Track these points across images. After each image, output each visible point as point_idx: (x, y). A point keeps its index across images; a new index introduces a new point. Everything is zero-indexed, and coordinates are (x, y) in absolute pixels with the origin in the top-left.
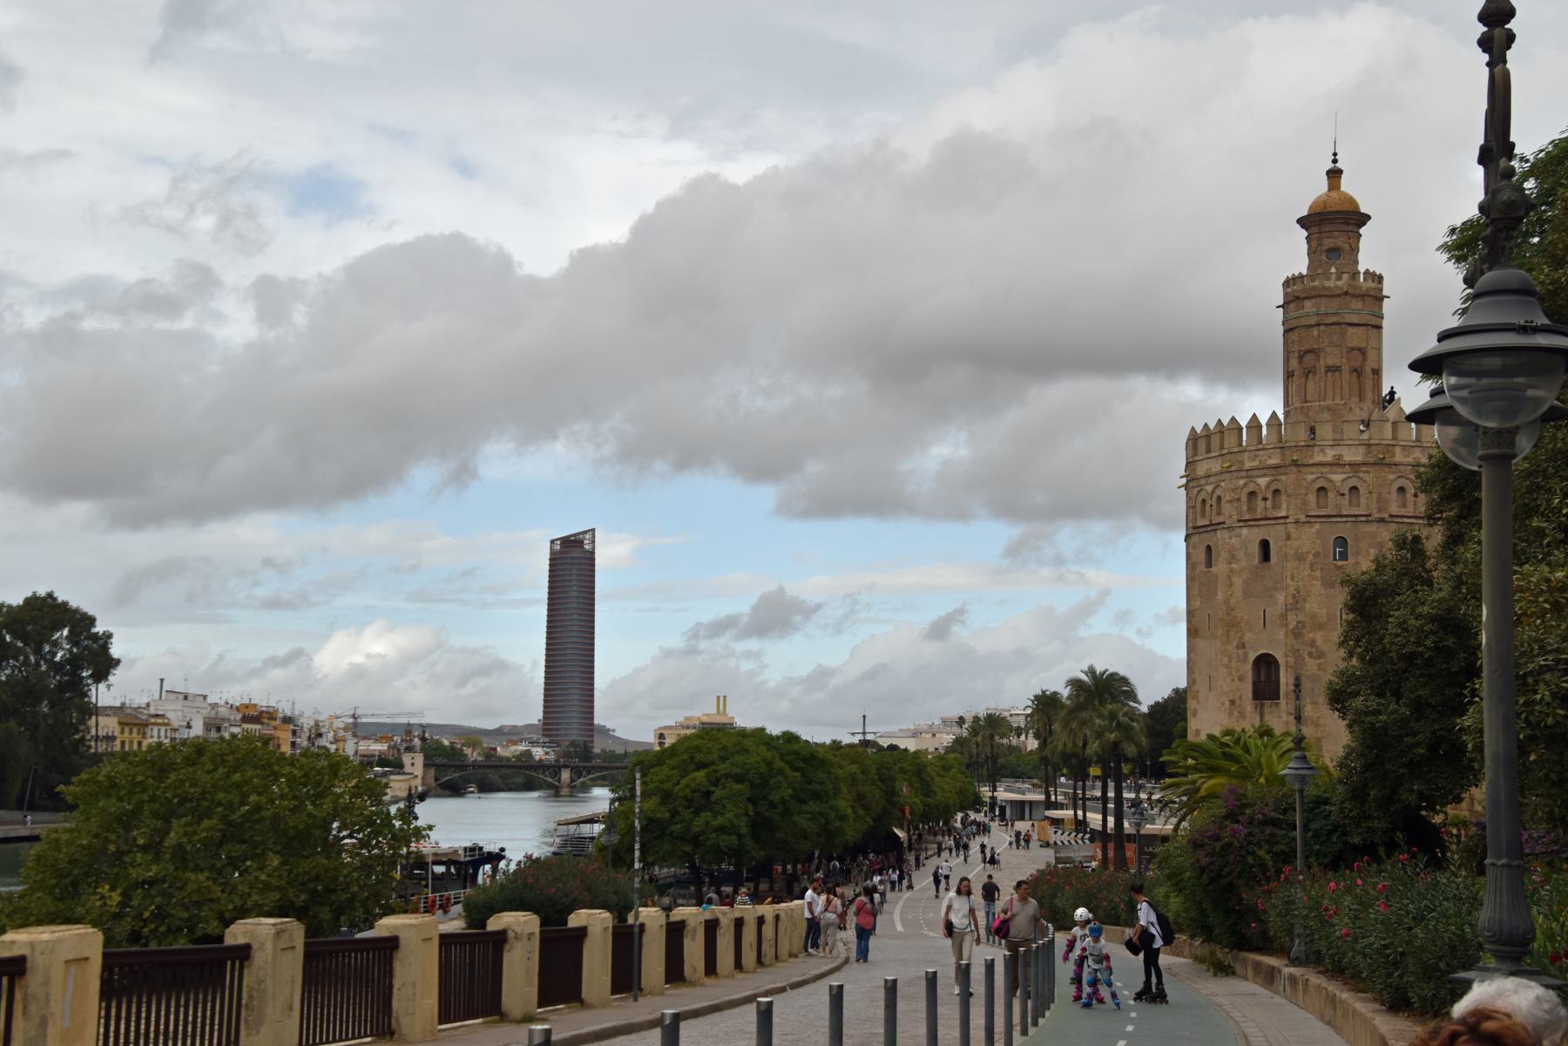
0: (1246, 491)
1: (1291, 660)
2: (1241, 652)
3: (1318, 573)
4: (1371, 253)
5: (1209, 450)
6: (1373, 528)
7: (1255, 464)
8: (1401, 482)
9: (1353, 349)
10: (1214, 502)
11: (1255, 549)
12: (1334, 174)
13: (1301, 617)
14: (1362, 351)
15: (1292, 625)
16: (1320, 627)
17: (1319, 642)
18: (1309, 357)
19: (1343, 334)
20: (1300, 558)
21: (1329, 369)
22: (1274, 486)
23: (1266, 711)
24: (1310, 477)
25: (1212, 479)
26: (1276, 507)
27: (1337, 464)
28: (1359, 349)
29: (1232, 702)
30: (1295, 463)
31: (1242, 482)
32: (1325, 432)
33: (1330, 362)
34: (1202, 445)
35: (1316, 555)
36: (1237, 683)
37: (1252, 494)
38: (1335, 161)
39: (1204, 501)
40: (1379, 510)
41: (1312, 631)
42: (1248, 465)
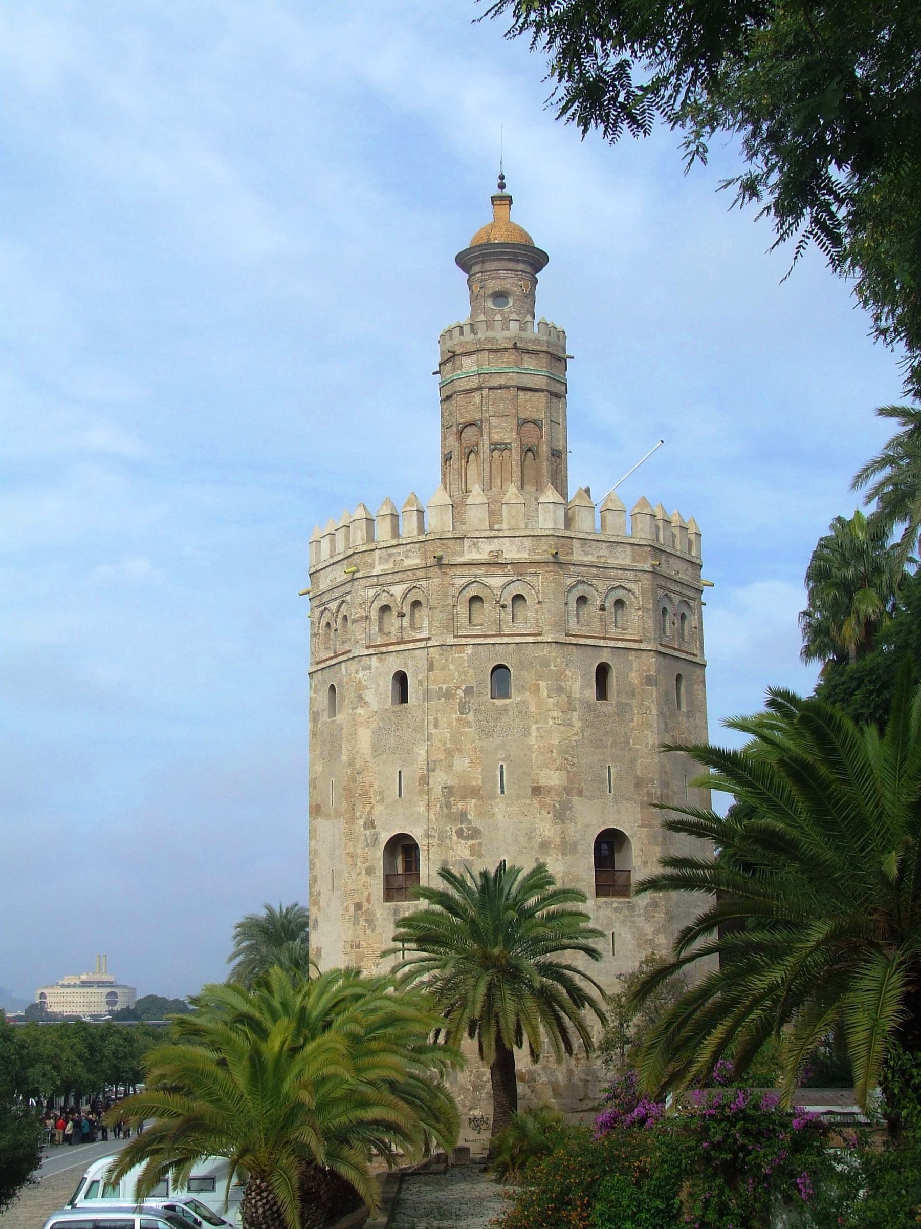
0: (377, 605)
1: (434, 842)
2: (368, 832)
3: (470, 717)
7: (389, 566)
8: (580, 590)
9: (526, 422)
11: (387, 684)
12: (503, 200)
15: (437, 790)
18: (470, 432)
20: (448, 695)
21: (496, 447)
22: (412, 597)
24: (460, 582)
25: (337, 593)
27: (494, 564)
28: (534, 422)
29: (358, 906)
31: (372, 592)
32: (476, 517)
33: (496, 437)
35: (469, 691)
36: (364, 878)
37: (385, 609)
38: (502, 186)
41: (463, 798)
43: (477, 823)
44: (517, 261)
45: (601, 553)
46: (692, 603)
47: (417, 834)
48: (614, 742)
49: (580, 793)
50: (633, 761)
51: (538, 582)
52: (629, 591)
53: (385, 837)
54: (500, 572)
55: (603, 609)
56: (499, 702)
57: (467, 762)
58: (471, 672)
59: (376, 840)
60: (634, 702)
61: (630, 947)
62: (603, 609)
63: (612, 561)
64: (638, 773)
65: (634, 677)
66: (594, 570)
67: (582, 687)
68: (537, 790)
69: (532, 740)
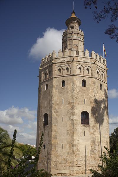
3: (57, 90)
8: (80, 66)
16: (58, 104)
19: (72, 42)
23: (45, 128)
24: (57, 66)
41: (56, 105)
43: (58, 110)
44: (75, 21)
45: (84, 60)
46: (104, 72)
47: (48, 113)
48: (86, 95)
49: (78, 104)
50: (90, 99)
52: (90, 67)
53: (44, 114)
54: (64, 64)
55: (84, 70)
56: (63, 87)
57: (56, 99)
58: (58, 82)
59: (42, 115)
60: (90, 87)
61: (88, 134)
62: (84, 70)
63: (86, 61)
64: (91, 101)
65: (90, 82)
66: (82, 63)
68: (69, 103)
69: (69, 94)
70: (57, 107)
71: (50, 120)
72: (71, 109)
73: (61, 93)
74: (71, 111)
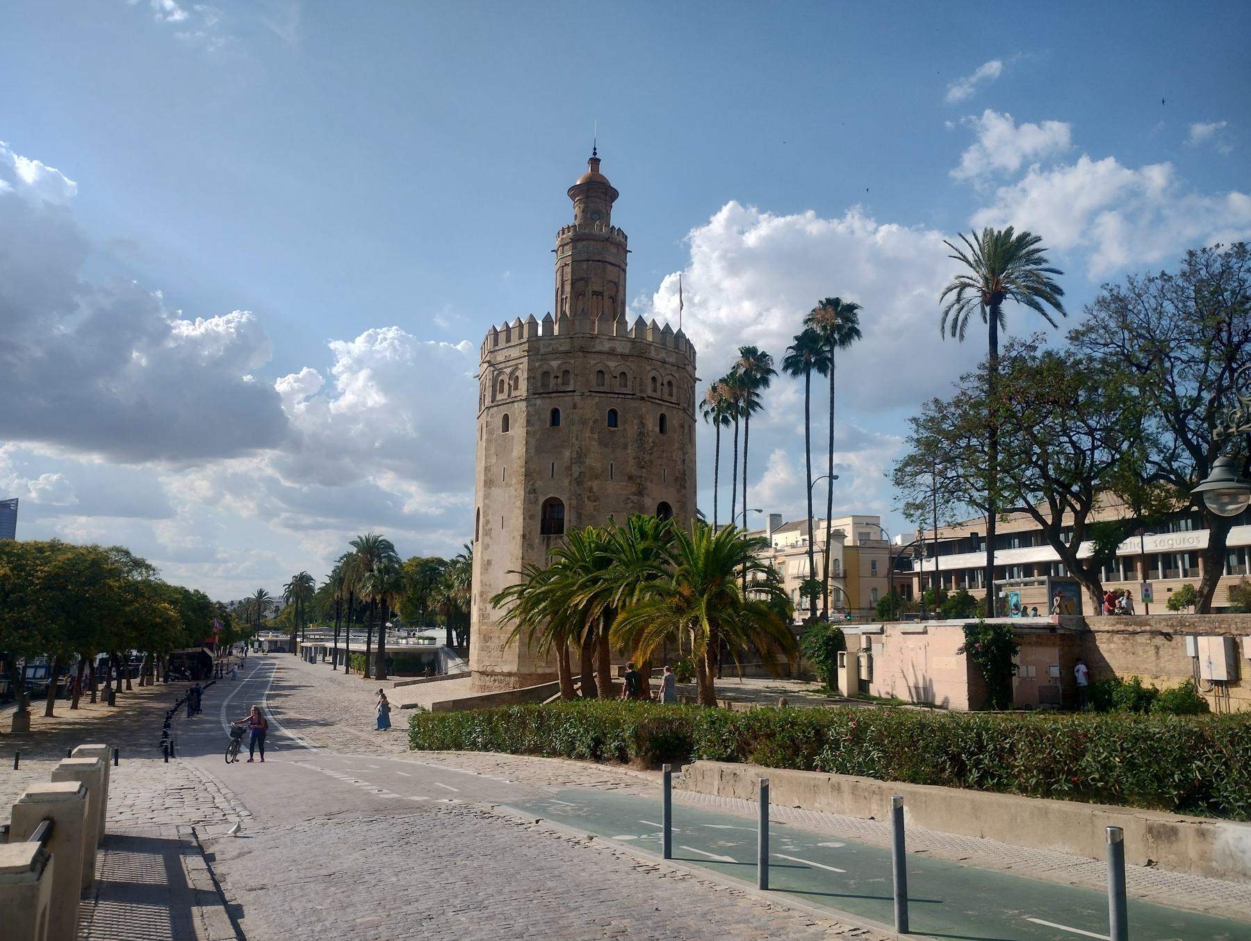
1: (574, 502)
3: (596, 436)
4: (619, 216)
5: (508, 340)
6: (637, 404)
10: (512, 383)
12: (595, 162)
13: (582, 469)
14: (616, 285)
16: (597, 477)
17: (595, 489)
20: (584, 423)
21: (594, 293)
22: (564, 368)
23: (552, 543)
24: (593, 362)
26: (565, 383)
29: (524, 536)
30: (582, 349)
33: (596, 289)
34: (502, 337)
37: (546, 374)
38: (595, 154)
39: (502, 381)
40: (641, 391)
42: (542, 351)
51: (633, 366)
53: (542, 500)
67: (652, 425)
68: (630, 478)
70: (595, 484)
71: (573, 519)
72: (634, 494)
73: (606, 446)
74: (635, 498)
